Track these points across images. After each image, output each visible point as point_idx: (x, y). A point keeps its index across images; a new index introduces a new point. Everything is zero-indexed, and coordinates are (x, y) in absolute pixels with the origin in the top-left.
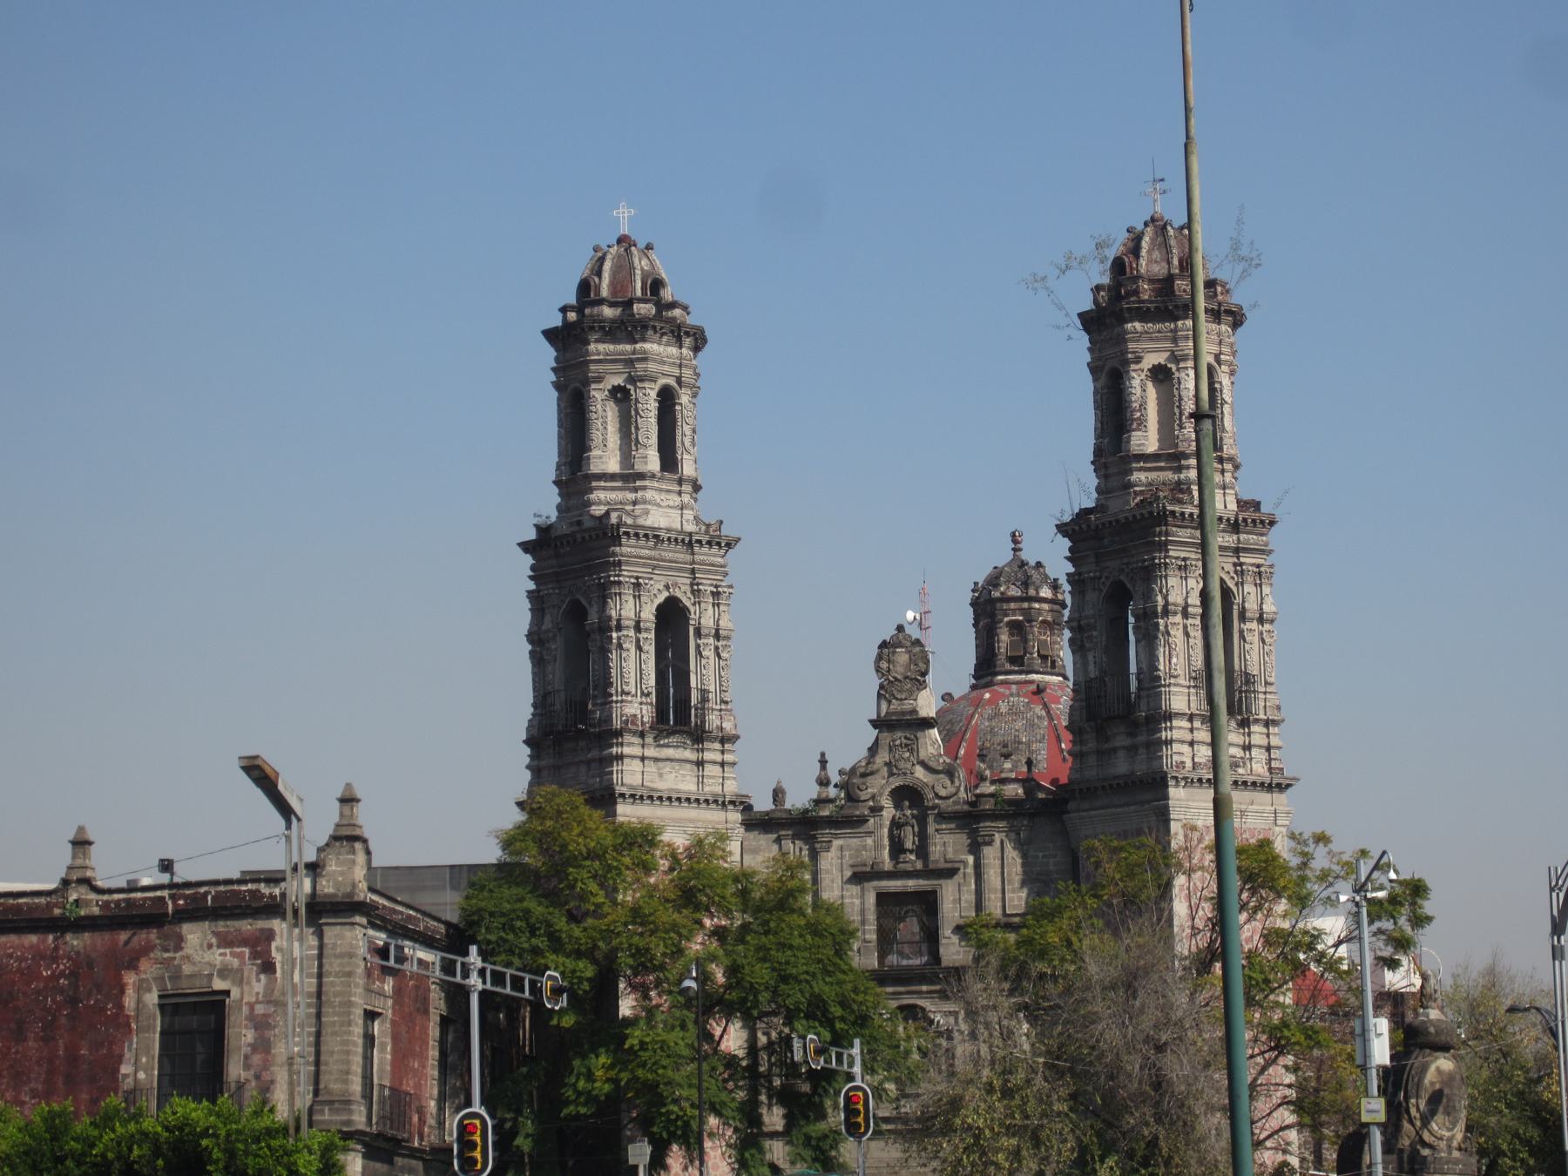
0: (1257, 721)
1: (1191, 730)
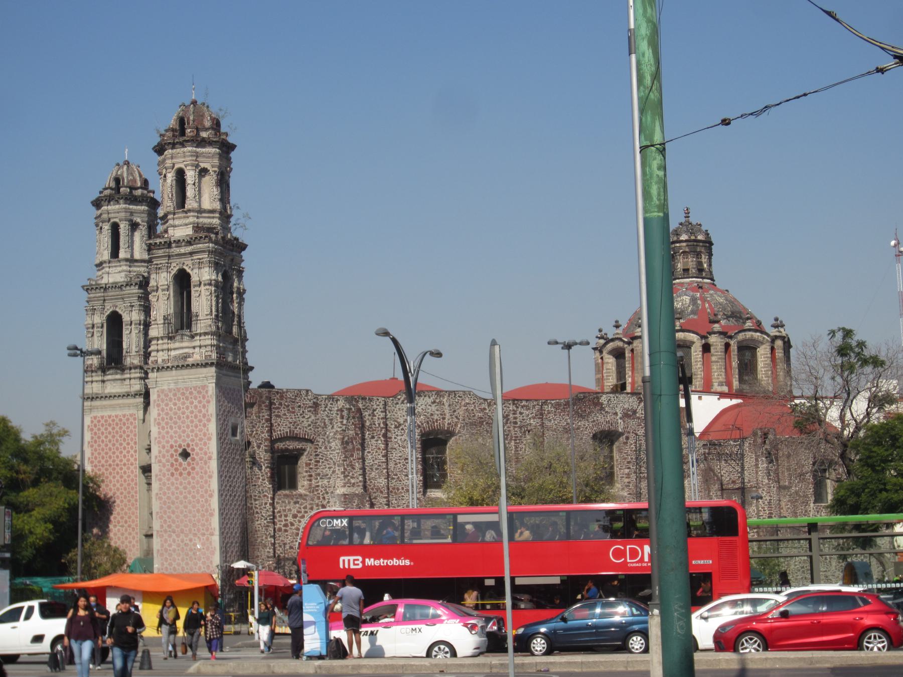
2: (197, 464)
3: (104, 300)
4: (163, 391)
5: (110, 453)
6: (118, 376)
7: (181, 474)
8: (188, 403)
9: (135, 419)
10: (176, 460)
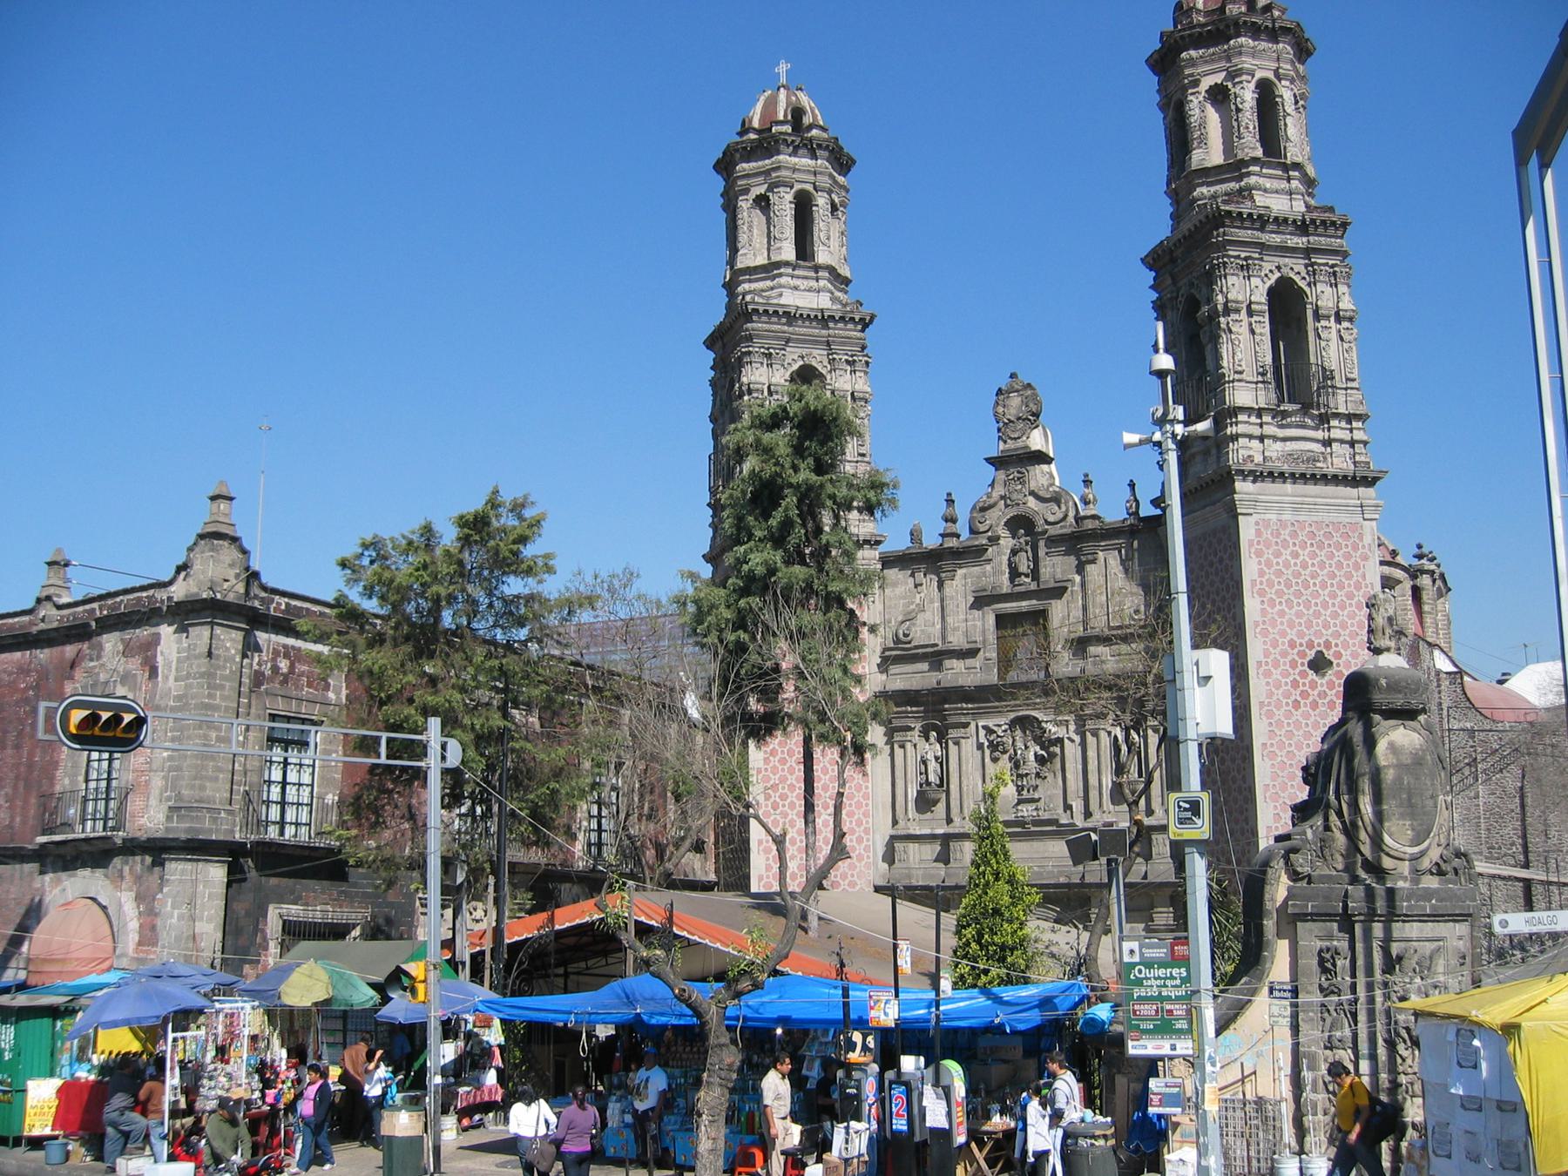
0: (1336, 416)
1: (1261, 425)
3: (788, 341)
4: (1267, 523)
7: (1314, 705)
8: (1322, 555)
10: (1303, 674)
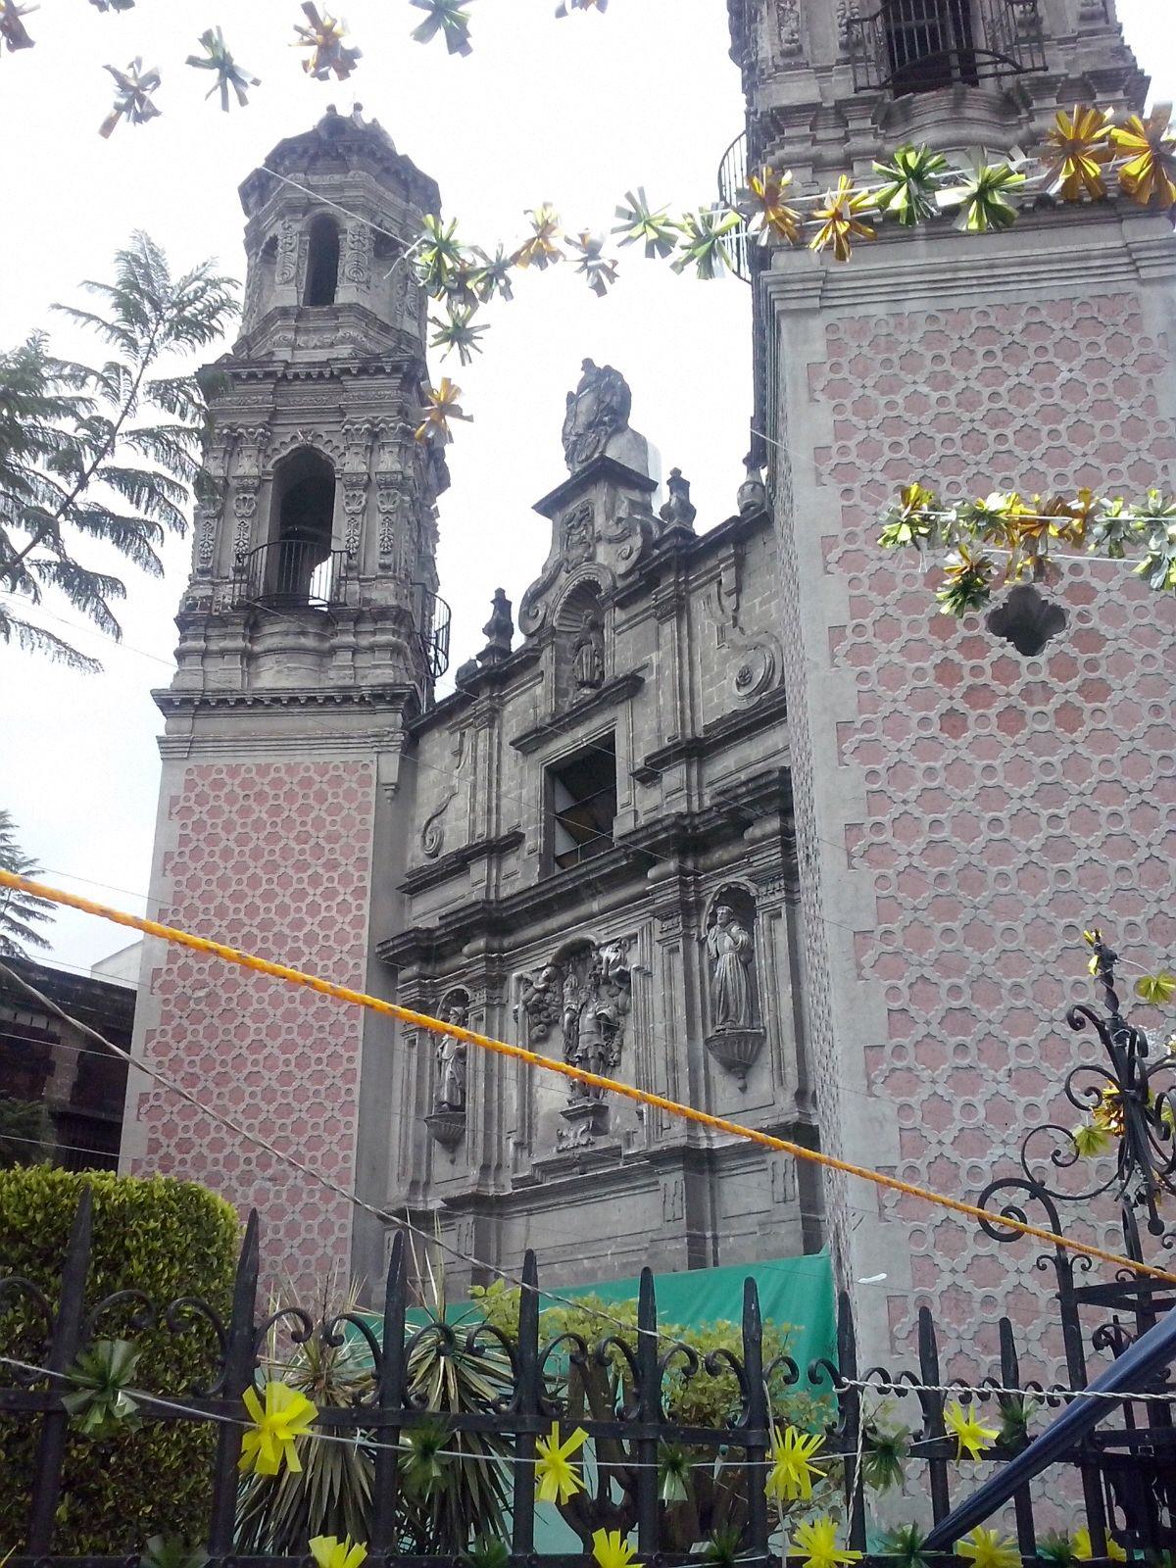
2: (1121, 663)
3: (274, 414)
5: (254, 897)
6: (309, 642)
9: (364, 782)
